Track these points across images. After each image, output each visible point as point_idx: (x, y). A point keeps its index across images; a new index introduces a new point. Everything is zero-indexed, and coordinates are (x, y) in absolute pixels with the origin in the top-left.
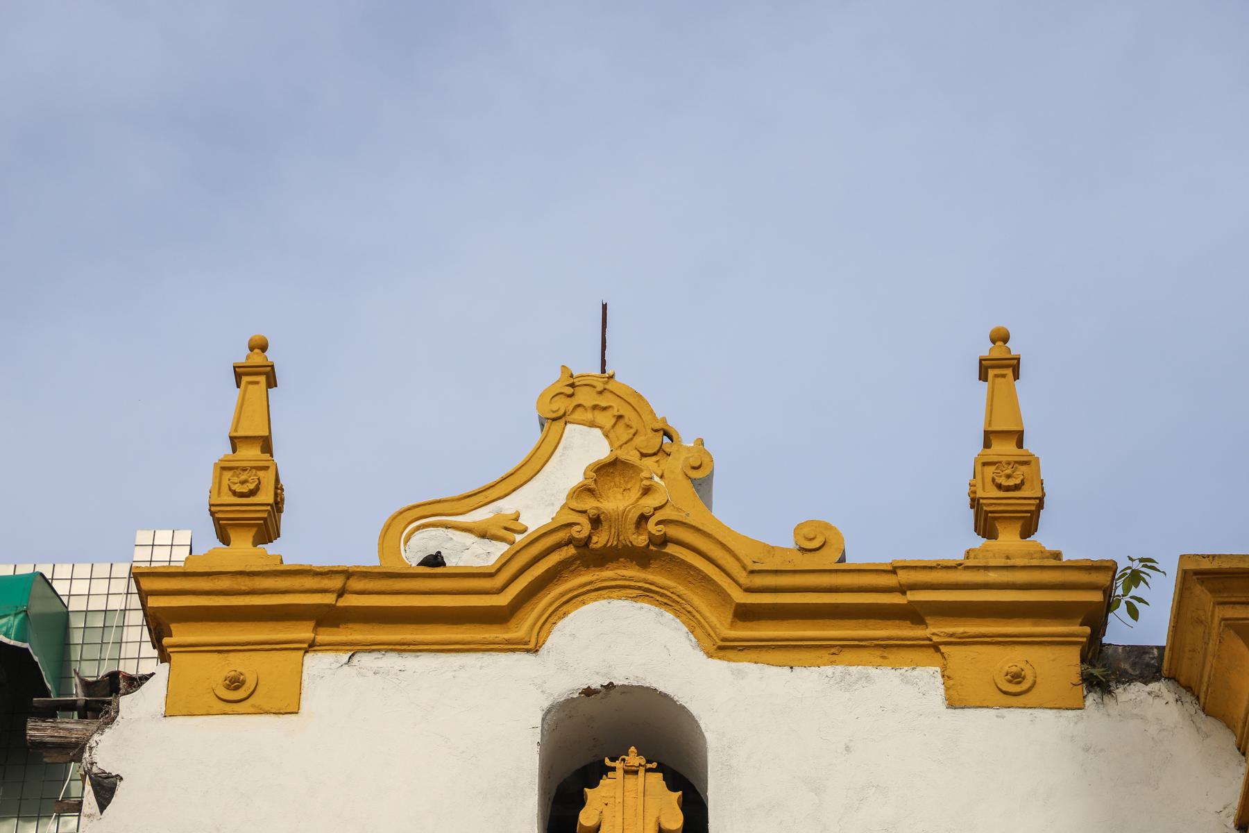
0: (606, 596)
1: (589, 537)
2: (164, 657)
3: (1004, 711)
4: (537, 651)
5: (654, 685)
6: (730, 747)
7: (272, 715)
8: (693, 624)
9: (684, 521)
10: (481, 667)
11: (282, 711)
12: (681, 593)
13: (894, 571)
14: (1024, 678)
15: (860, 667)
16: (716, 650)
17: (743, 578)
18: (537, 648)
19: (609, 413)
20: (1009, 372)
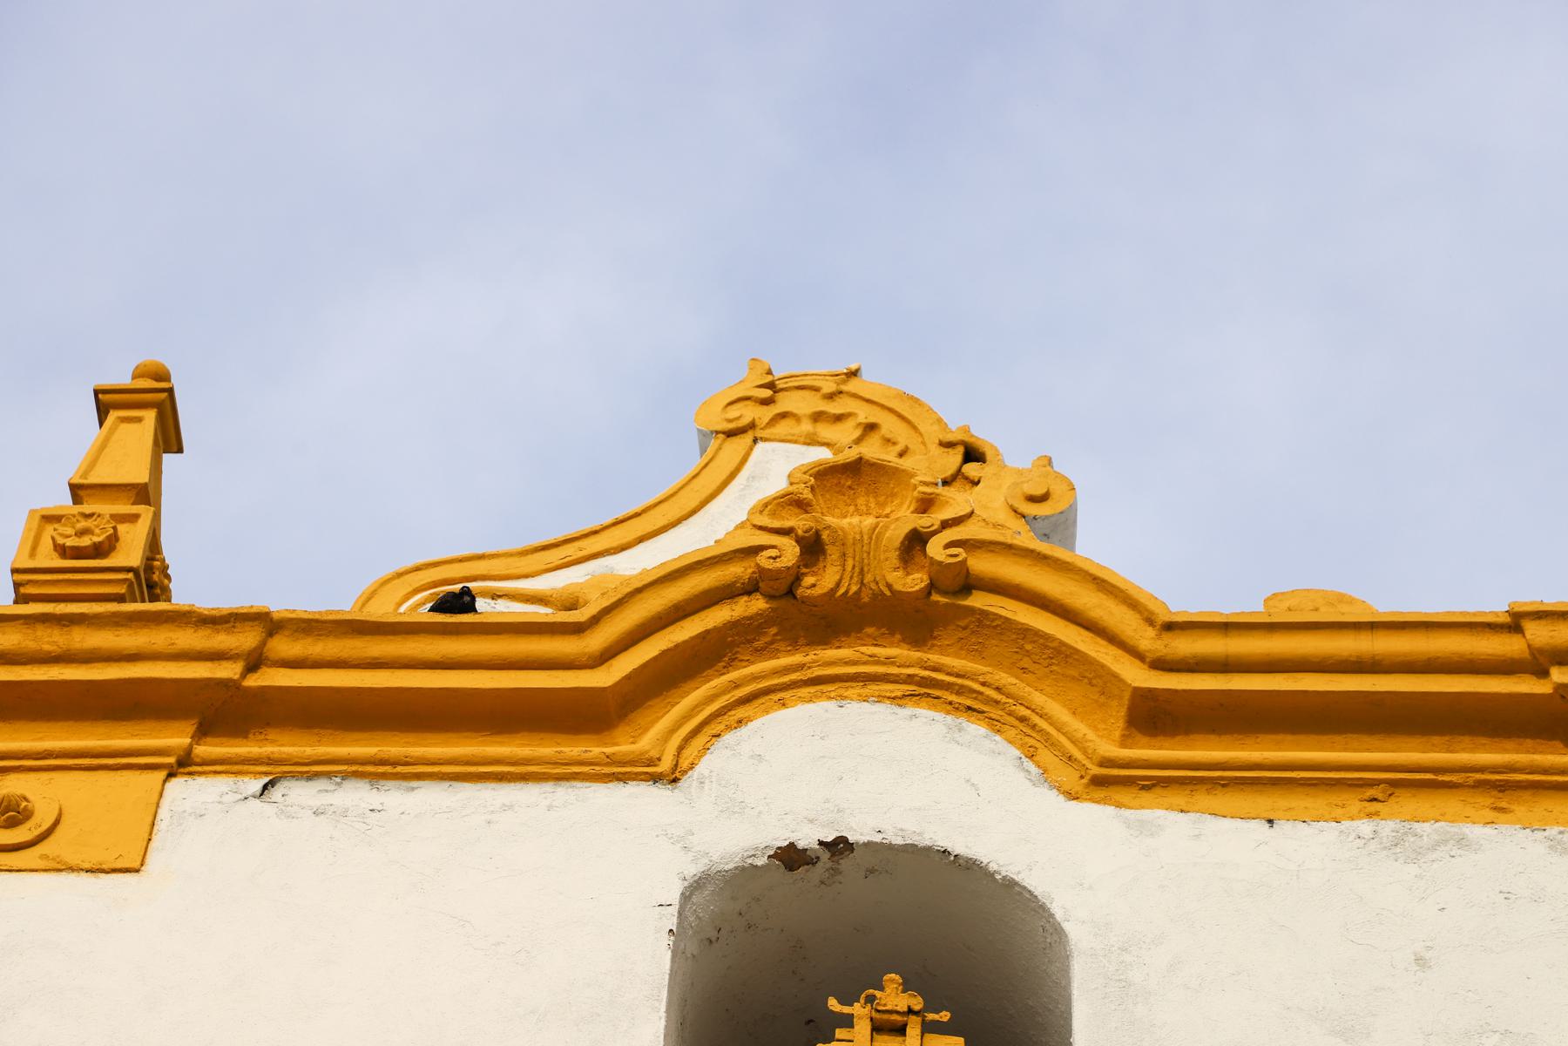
0: (832, 694)
1: (798, 579)
4: (675, 780)
5: (942, 842)
6: (1125, 950)
8: (1032, 742)
9: (1009, 541)
10: (549, 808)
12: (1003, 682)
16: (1087, 786)
17: (1147, 640)
18: (677, 774)
19: (849, 424)
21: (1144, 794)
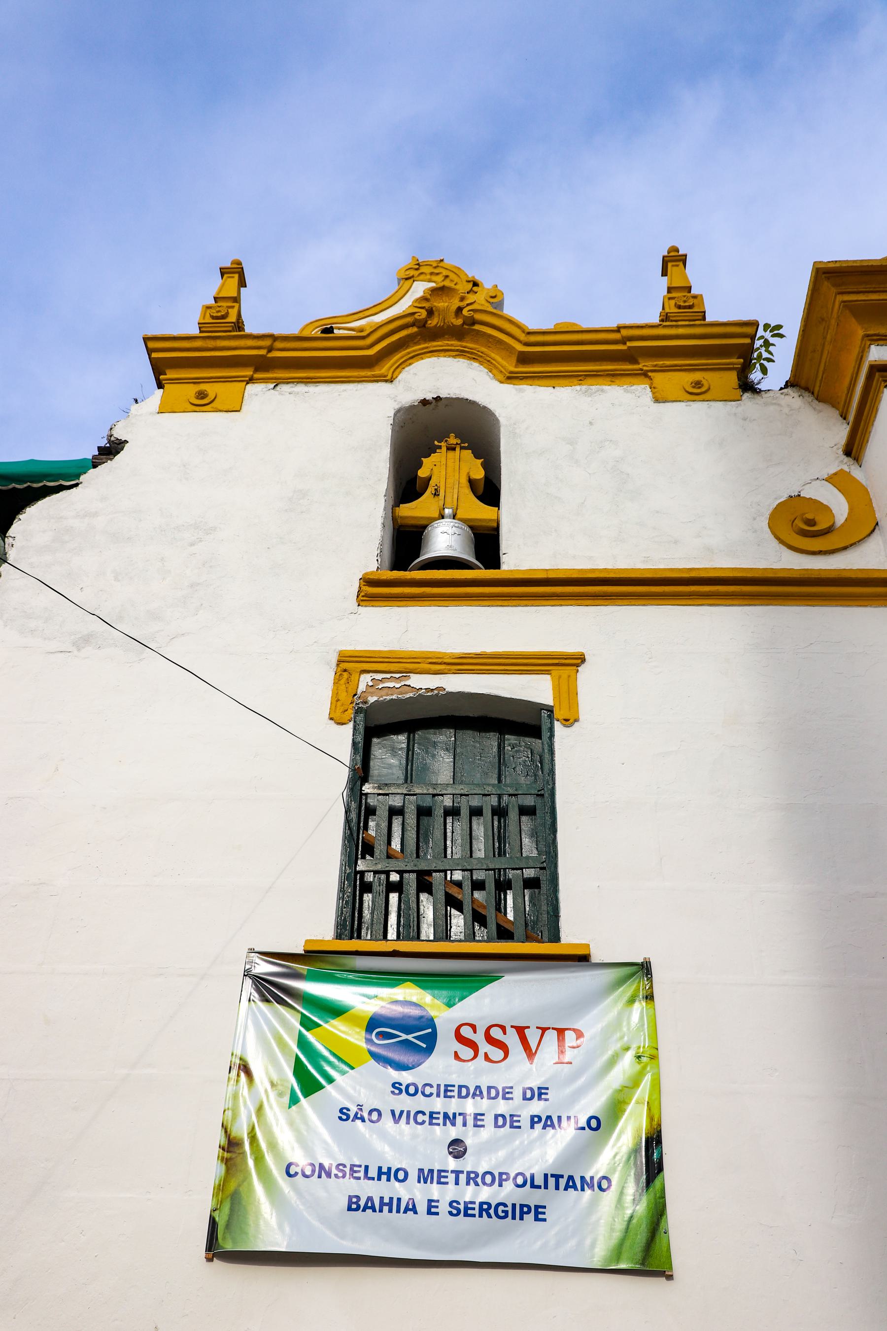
1: (426, 322)
2: (160, 386)
3: (691, 403)
4: (392, 381)
5: (466, 397)
6: (515, 424)
7: (224, 412)
8: (491, 367)
9: (485, 309)
10: (356, 390)
11: (230, 410)
13: (618, 329)
15: (597, 386)
16: (506, 379)
17: (523, 337)
20: (681, 264)
21: (520, 381)
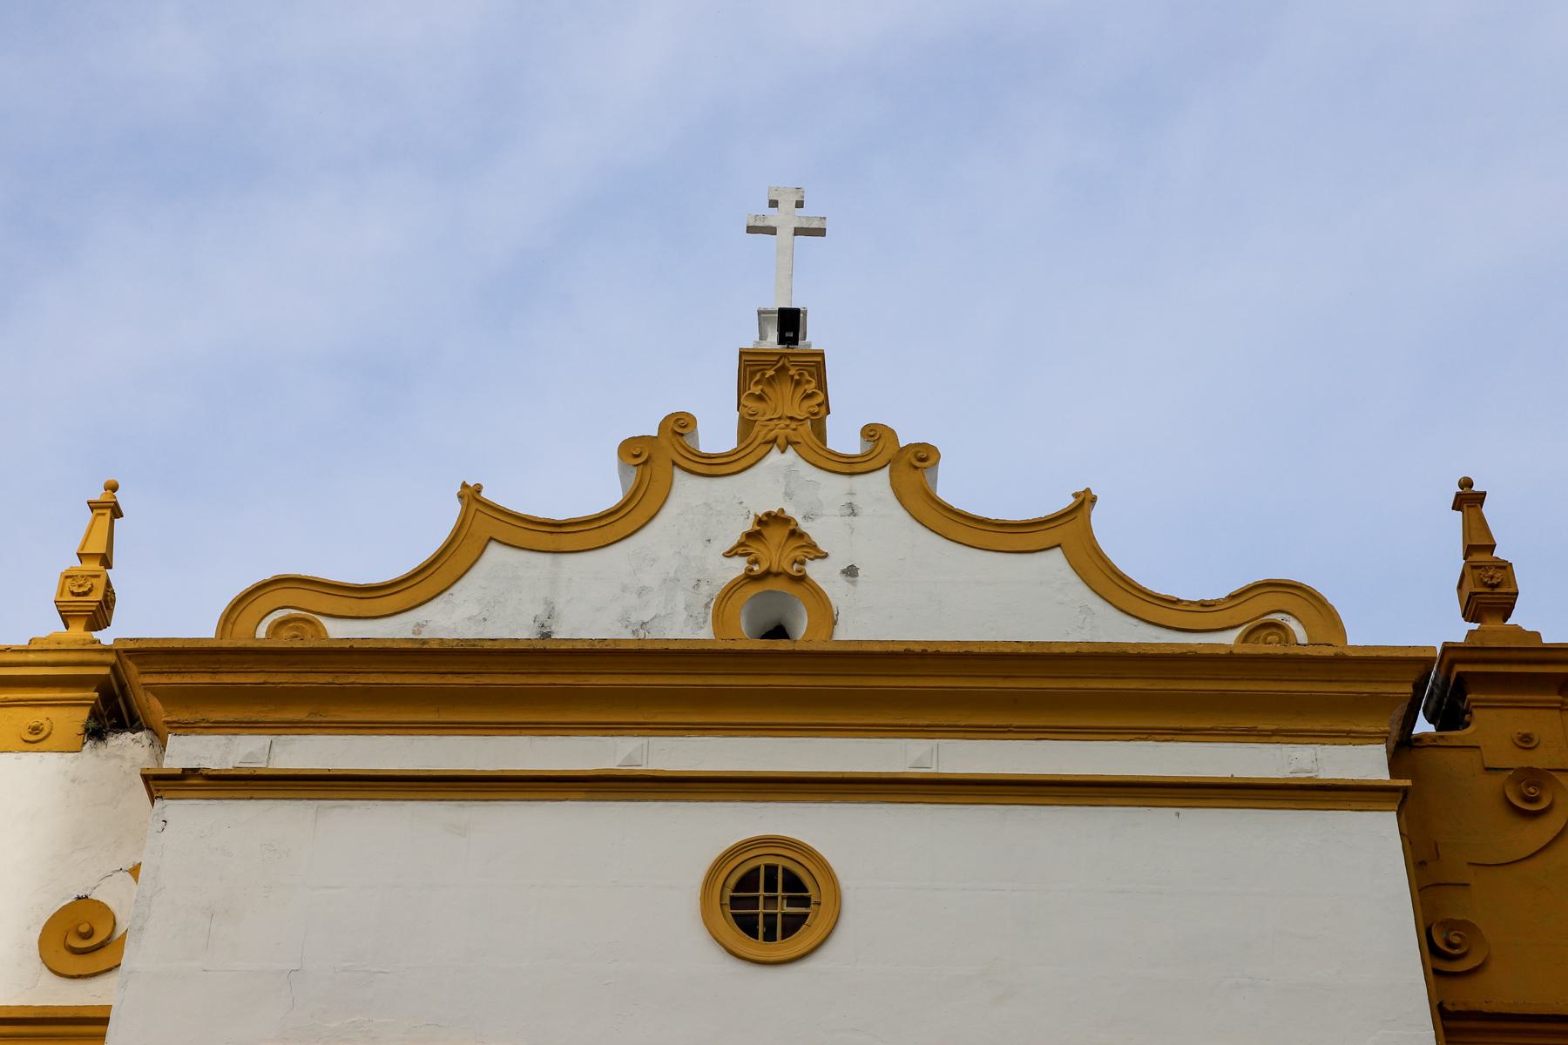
14: (42, 730)
